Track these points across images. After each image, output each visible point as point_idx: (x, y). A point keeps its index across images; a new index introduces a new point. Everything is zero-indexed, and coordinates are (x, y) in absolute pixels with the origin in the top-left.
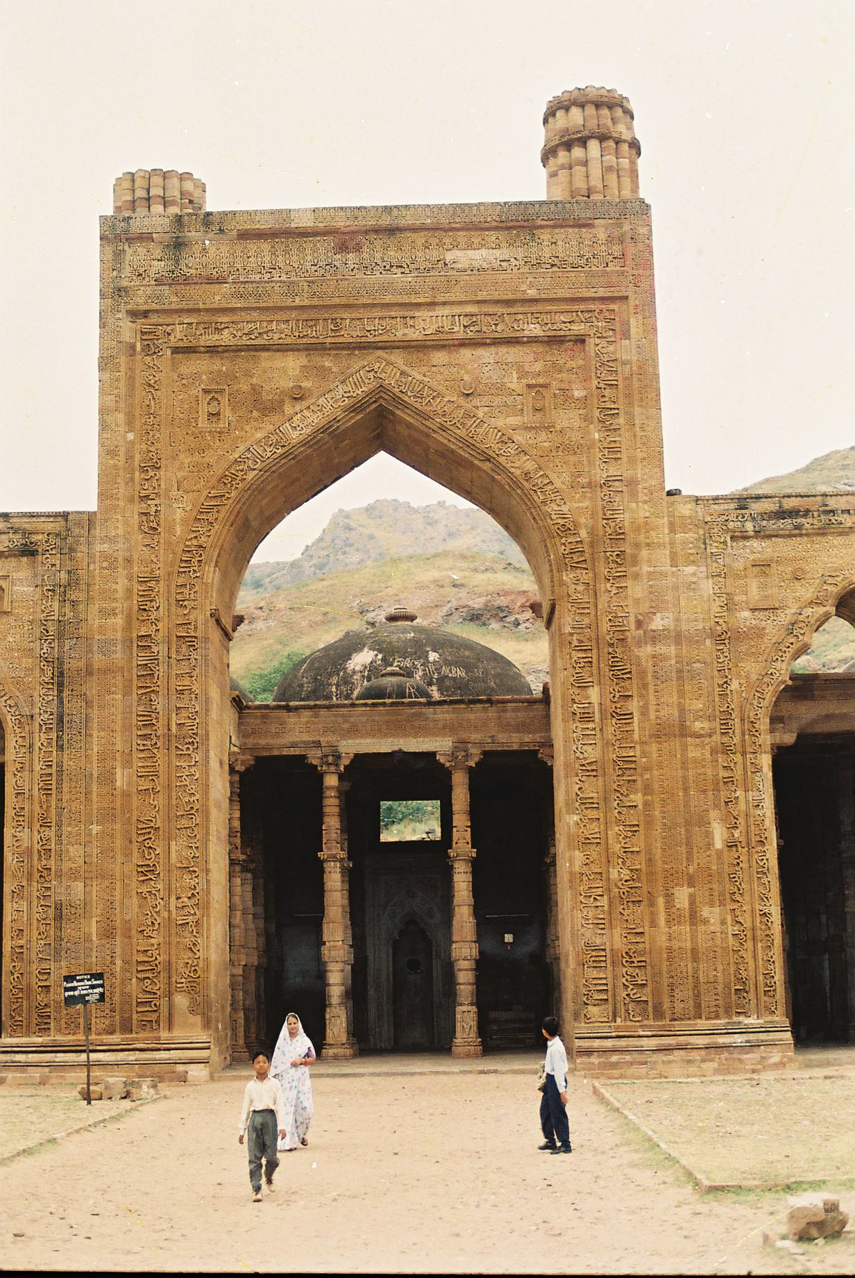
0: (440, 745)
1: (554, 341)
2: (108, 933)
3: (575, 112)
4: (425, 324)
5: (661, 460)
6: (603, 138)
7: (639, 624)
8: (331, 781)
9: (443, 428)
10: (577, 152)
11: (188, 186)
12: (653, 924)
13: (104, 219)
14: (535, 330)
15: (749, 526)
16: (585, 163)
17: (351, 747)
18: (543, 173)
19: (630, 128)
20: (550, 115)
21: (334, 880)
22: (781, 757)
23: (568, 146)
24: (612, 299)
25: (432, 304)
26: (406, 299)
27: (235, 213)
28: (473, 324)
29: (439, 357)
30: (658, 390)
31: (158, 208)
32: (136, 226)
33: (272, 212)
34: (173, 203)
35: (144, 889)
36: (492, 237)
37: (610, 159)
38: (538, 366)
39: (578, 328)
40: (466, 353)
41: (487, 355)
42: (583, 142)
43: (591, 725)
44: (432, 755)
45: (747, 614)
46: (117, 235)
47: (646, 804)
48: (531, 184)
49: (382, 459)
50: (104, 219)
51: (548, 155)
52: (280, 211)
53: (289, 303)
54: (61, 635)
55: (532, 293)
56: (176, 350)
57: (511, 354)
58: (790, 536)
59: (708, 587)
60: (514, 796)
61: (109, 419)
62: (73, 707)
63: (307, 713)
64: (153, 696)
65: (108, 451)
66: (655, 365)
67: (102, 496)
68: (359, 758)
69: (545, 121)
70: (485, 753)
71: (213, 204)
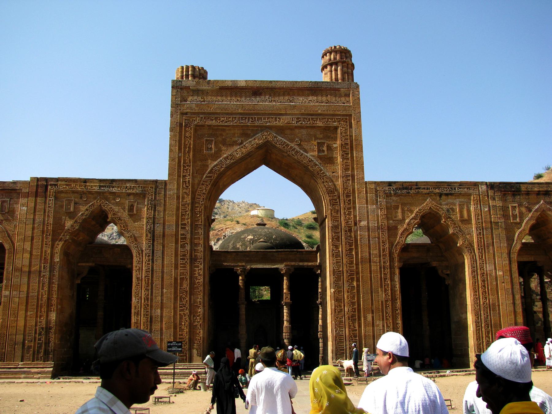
1: (326, 129)
2: (168, 328)
4: (282, 121)
5: (363, 169)
6: (343, 62)
7: (355, 224)
9: (289, 155)
11: (202, 72)
12: (360, 326)
13: (173, 81)
15: (392, 192)
16: (336, 70)
19: (351, 60)
20: (325, 54)
21: (243, 311)
22: (401, 270)
23: (331, 65)
24: (347, 115)
25: (286, 114)
26: (277, 112)
27: (218, 81)
28: (300, 121)
29: (288, 132)
30: (362, 145)
32: (184, 84)
33: (231, 81)
34: (197, 77)
35: (182, 313)
36: (307, 92)
37: (345, 69)
38: (321, 136)
39: (335, 124)
40: (297, 131)
41: (304, 132)
43: (339, 258)
44: (277, 269)
46: (177, 86)
47: (358, 286)
49: (263, 169)
50: (173, 81)
52: (234, 81)
53: (236, 111)
54: (154, 223)
56: (196, 126)
57: (312, 132)
58: (406, 196)
60: (307, 282)
61: (172, 148)
62: (158, 248)
63: (234, 254)
64: (186, 245)
65: (171, 159)
66: (361, 138)
67: (170, 175)
68: (252, 269)
69: (323, 57)
70: (295, 269)
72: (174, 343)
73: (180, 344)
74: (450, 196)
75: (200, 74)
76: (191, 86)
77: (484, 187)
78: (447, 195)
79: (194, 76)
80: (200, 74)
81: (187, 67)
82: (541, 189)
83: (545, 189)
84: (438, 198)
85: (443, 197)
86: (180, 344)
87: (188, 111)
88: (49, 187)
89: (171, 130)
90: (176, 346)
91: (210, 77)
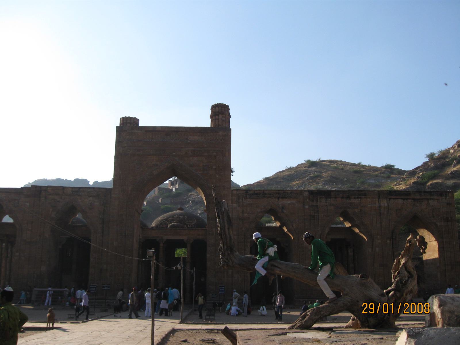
0: (185, 238)
3: (217, 108)
8: (161, 245)
10: (217, 117)
11: (136, 120)
13: (117, 127)
14: (206, 154)
17: (166, 238)
18: (209, 120)
31: (129, 125)
42: (218, 115)
44: (183, 240)
45: (246, 214)
46: (120, 130)
48: (207, 123)
50: (117, 127)
51: (211, 117)
59: (239, 208)
68: (168, 241)
71: (141, 124)
72: (106, 285)
73: (109, 286)
74: (284, 199)
75: (134, 122)
76: (128, 128)
77: (306, 194)
78: (282, 198)
79: (130, 123)
80: (135, 121)
84: (277, 200)
85: (280, 199)
86: (109, 286)
87: (126, 145)
88: (43, 192)
89: (116, 157)
90: (107, 287)
91: (141, 124)
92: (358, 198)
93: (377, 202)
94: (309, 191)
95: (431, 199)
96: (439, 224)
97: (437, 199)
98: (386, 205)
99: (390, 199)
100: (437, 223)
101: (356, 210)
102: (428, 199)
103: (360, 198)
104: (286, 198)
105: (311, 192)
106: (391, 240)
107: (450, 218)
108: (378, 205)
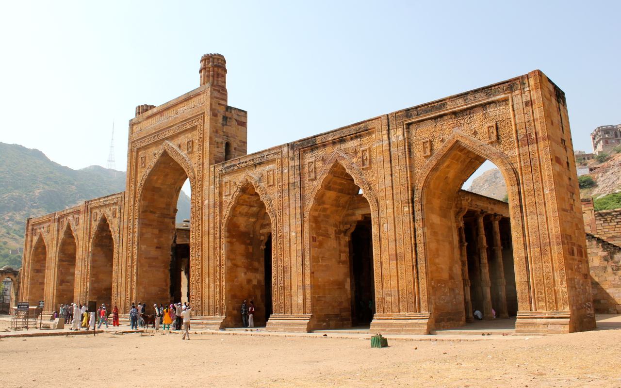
55: (189, 117)
77: (285, 149)
81: (139, 107)
82: (334, 138)
83: (339, 136)
92: (356, 137)
93: (385, 137)
94: (288, 145)
95: (489, 103)
96: (509, 153)
97: (506, 100)
98: (401, 138)
99: (409, 125)
100: (506, 152)
101: (355, 160)
102: (484, 106)
103: (360, 136)
104: (260, 164)
105: (291, 146)
106: (410, 205)
107: (534, 136)
108: (387, 142)
